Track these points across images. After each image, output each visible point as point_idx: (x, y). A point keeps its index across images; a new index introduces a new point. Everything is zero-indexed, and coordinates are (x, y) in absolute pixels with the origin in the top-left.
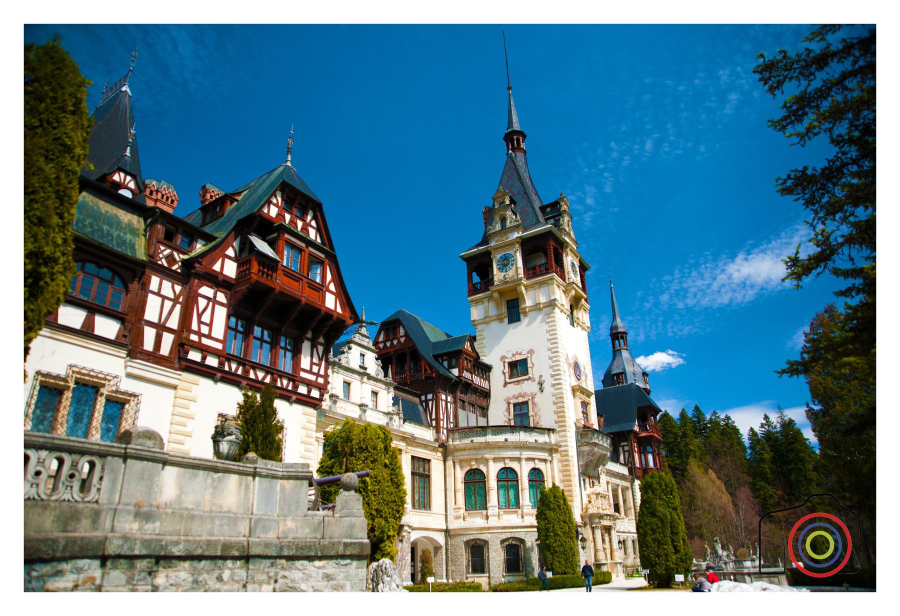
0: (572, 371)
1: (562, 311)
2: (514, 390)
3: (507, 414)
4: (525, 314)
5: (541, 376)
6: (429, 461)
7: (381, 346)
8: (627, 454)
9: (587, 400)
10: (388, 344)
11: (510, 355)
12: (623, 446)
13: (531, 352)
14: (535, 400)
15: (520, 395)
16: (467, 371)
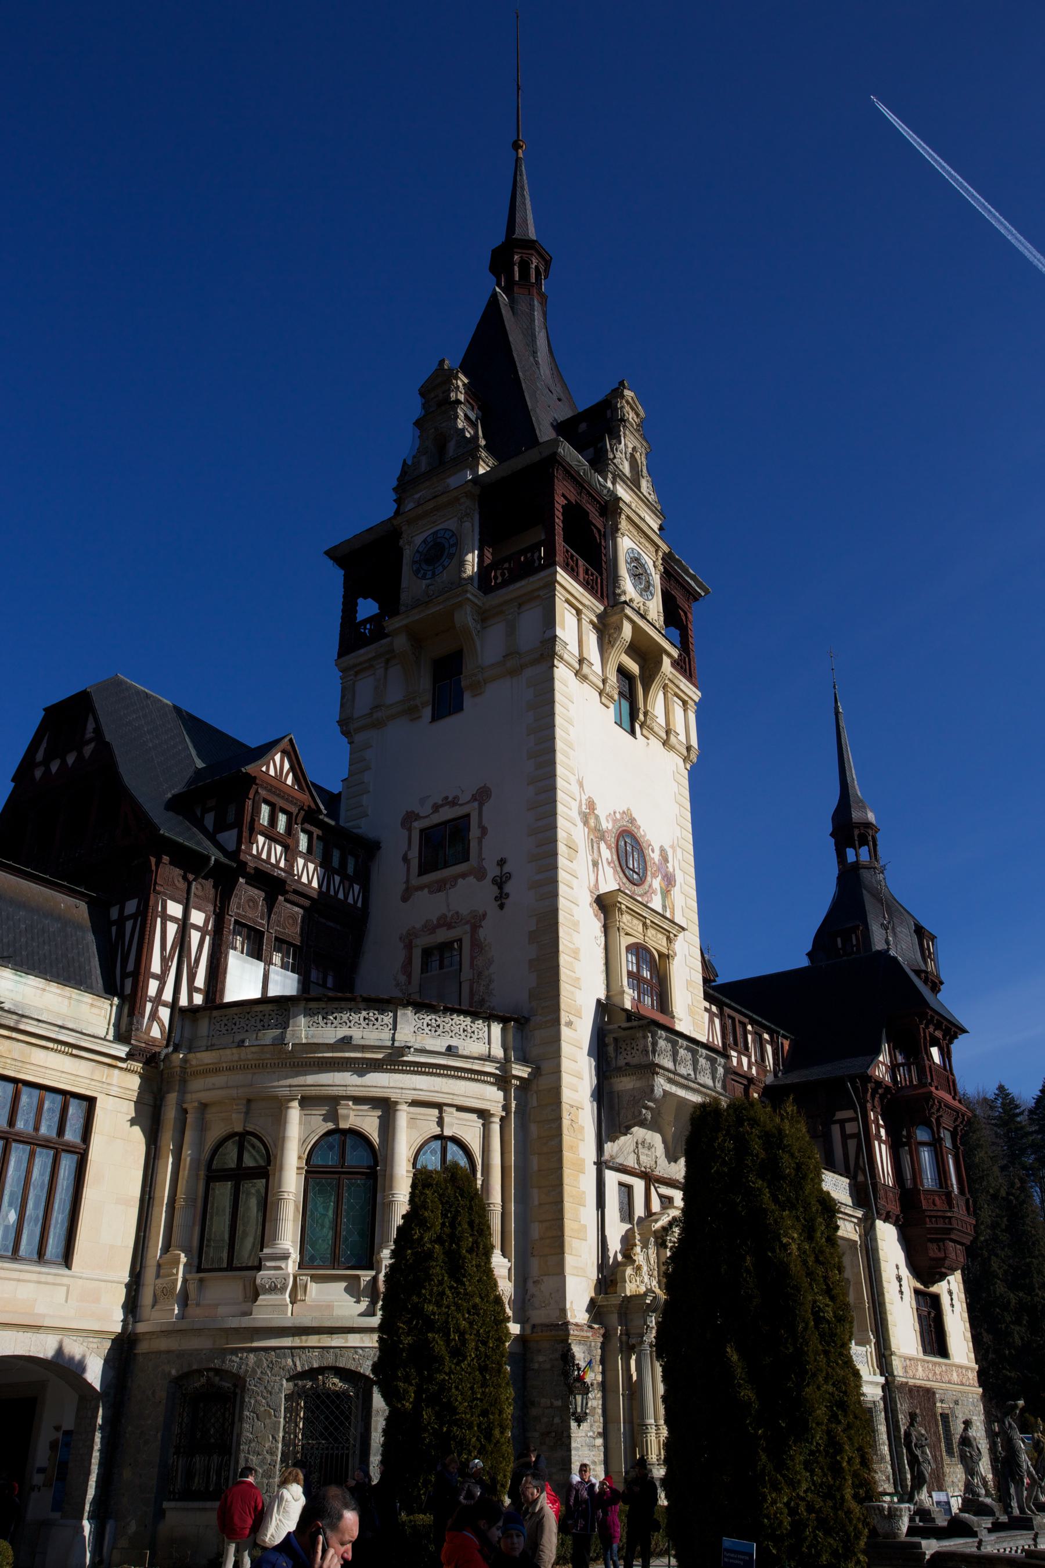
0: (606, 854)
2: (428, 907)
3: (403, 978)
4: (477, 688)
5: (502, 863)
6: (90, 1102)
7: (38, 773)
8: (852, 1144)
9: (656, 941)
10: (54, 767)
11: (427, 810)
12: (842, 1122)
13: (482, 795)
14: (482, 933)
15: (445, 922)
16: (272, 838)
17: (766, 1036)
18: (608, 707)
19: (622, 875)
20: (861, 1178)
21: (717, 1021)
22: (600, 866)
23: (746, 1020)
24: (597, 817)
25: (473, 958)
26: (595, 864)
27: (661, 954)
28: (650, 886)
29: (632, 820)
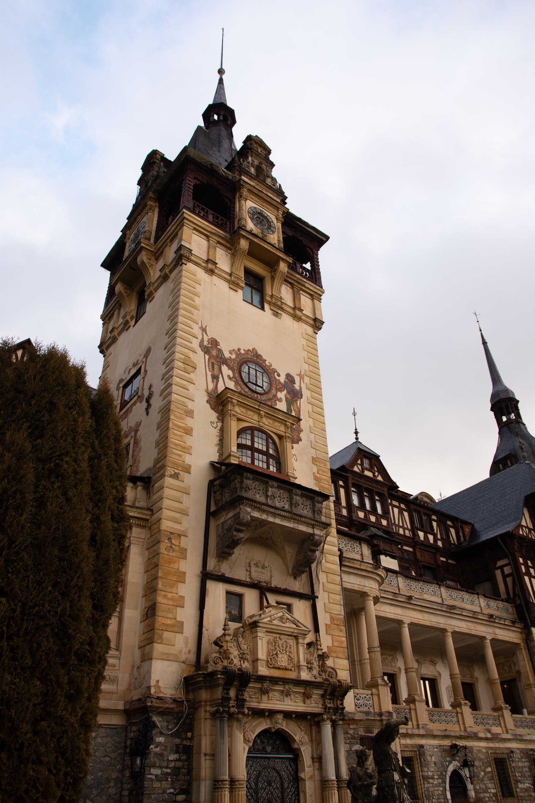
1: (211, 272)
8: (509, 580)
12: (501, 568)
14: (139, 433)
17: (449, 523)
18: (237, 291)
19: (244, 387)
20: (518, 602)
21: (406, 514)
22: (221, 379)
23: (431, 513)
24: (220, 351)
25: (134, 451)
26: (215, 378)
27: (280, 437)
28: (275, 396)
29: (259, 356)
